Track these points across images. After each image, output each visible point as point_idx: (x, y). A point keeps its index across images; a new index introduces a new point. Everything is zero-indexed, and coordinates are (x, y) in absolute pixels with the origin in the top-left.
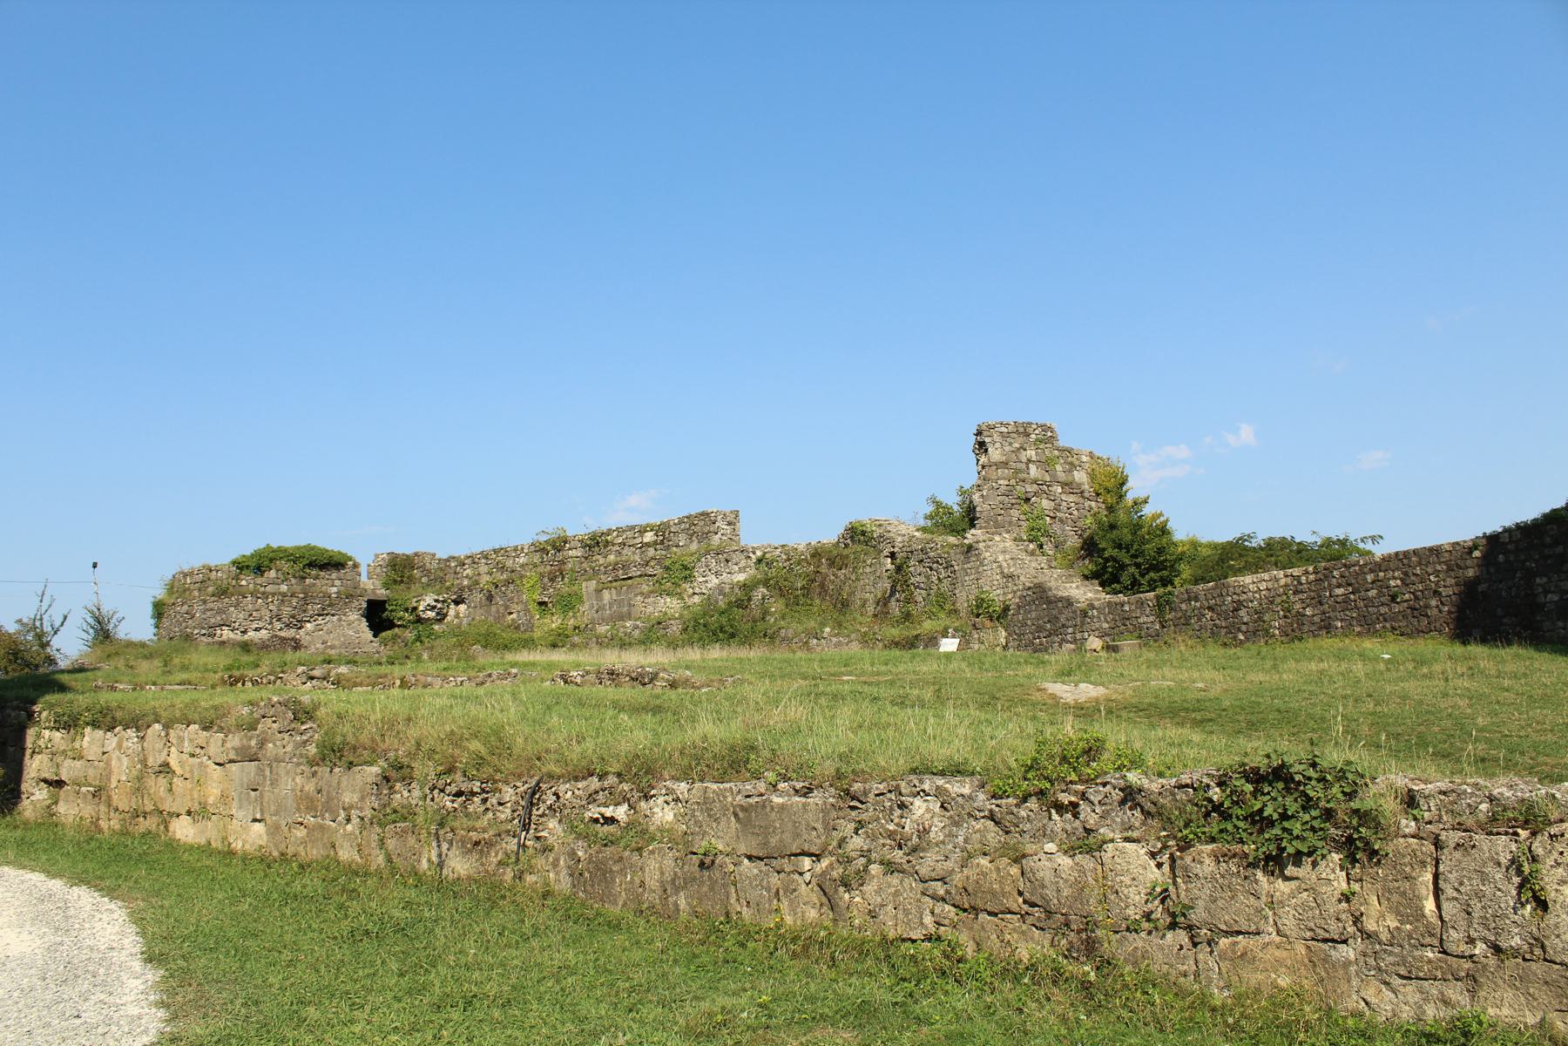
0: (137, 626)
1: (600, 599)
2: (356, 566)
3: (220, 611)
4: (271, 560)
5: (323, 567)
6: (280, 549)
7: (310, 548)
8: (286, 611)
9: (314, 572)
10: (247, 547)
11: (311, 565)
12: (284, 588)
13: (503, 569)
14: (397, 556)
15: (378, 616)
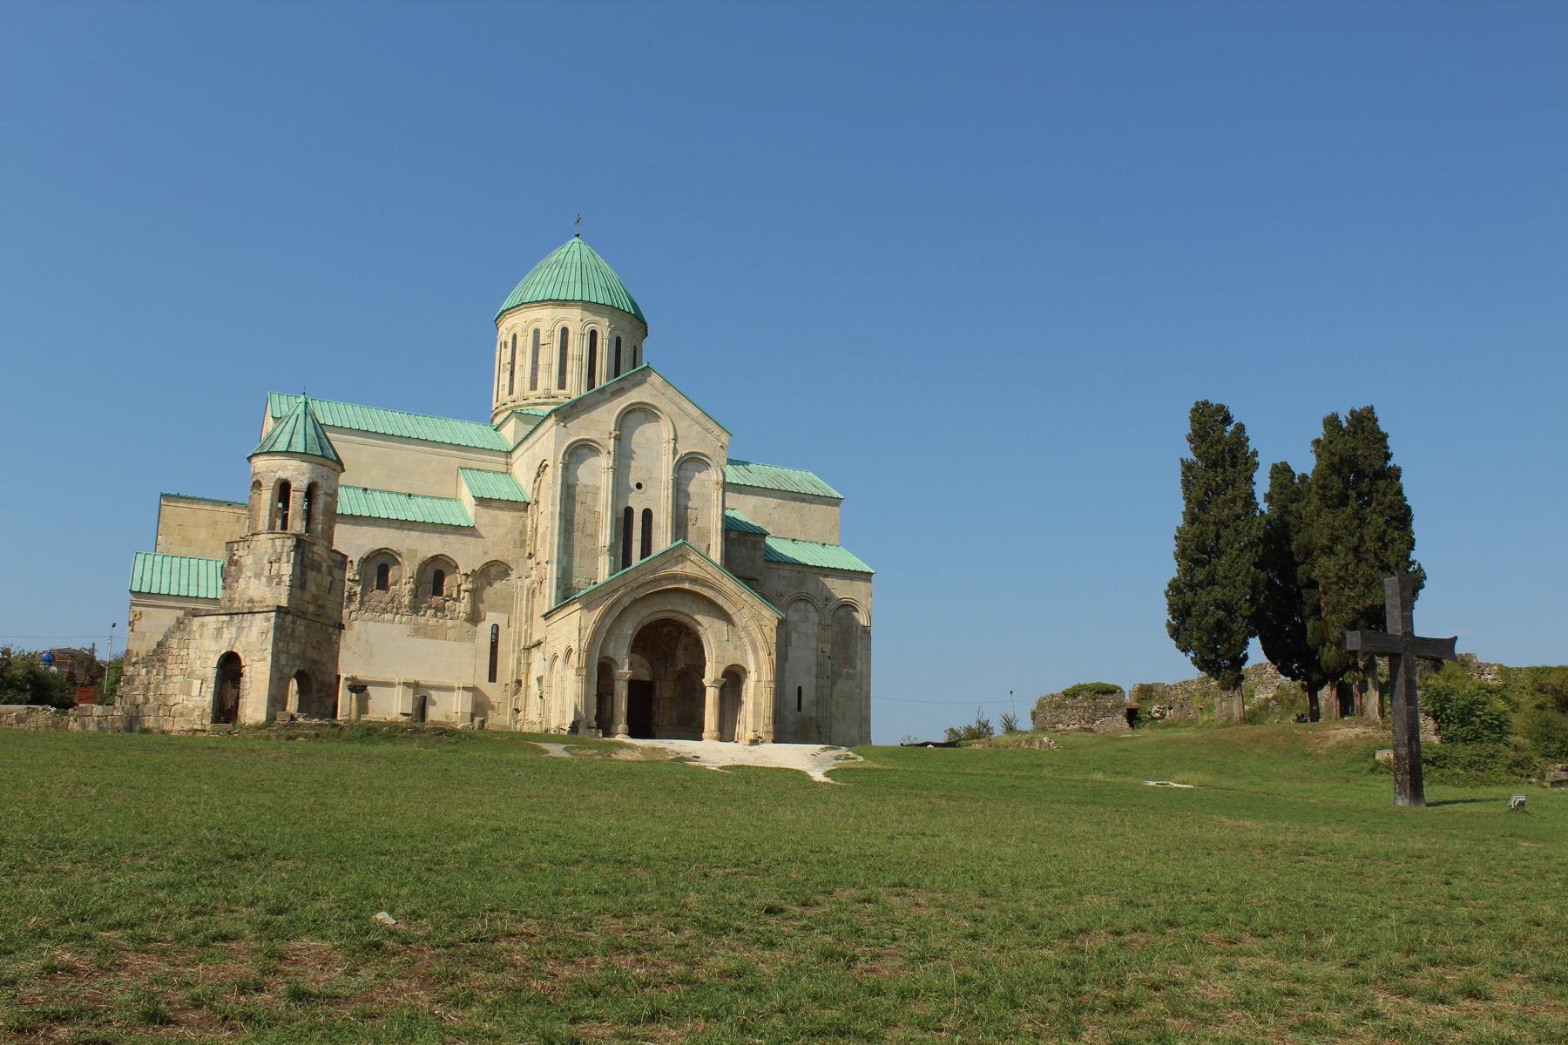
0: (1025, 723)
1: (1221, 706)
2: (1122, 691)
3: (1057, 716)
4: (1080, 691)
5: (1104, 693)
6: (1085, 686)
7: (1098, 684)
8: (1087, 715)
9: (1100, 696)
10: (1068, 685)
11: (1098, 692)
12: (1086, 704)
13: (1187, 691)
14: (1144, 685)
15: (1133, 717)
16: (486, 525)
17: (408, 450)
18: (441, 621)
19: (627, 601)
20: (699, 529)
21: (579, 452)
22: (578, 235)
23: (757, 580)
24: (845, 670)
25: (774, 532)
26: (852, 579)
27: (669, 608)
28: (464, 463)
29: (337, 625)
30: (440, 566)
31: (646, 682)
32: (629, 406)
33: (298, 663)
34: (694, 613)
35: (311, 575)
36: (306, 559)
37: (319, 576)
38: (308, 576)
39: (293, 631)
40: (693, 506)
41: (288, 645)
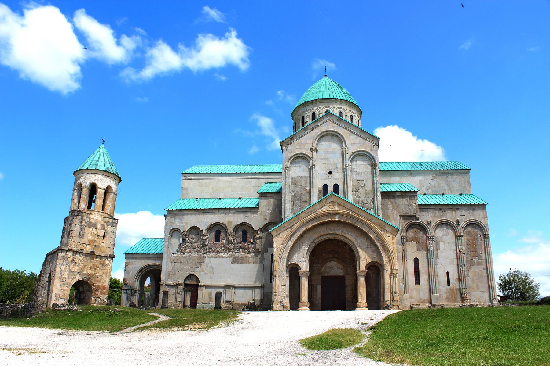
16: (265, 206)
17: (242, 178)
18: (246, 254)
19: (301, 231)
20: (366, 190)
21: (296, 160)
22: (326, 76)
23: (415, 216)
24: (475, 260)
25: (433, 191)
26: (473, 210)
27: (329, 232)
28: (267, 180)
29: (108, 256)
30: (245, 228)
31: (343, 276)
32: (321, 134)
33: (78, 276)
34: (345, 233)
35: (89, 231)
36: (84, 222)
37: (95, 230)
38: (86, 231)
39: (73, 260)
40: (362, 179)
41: (69, 267)
